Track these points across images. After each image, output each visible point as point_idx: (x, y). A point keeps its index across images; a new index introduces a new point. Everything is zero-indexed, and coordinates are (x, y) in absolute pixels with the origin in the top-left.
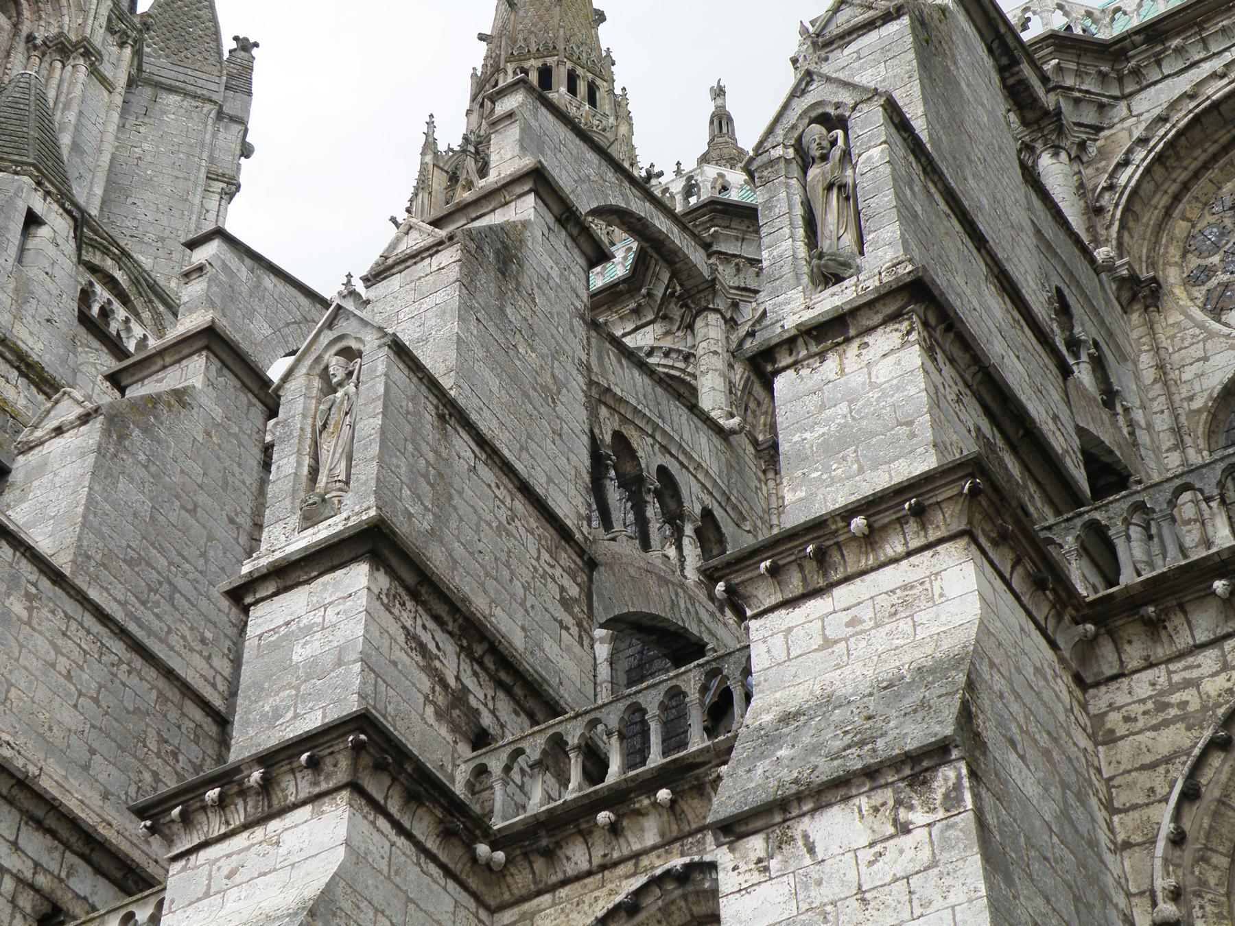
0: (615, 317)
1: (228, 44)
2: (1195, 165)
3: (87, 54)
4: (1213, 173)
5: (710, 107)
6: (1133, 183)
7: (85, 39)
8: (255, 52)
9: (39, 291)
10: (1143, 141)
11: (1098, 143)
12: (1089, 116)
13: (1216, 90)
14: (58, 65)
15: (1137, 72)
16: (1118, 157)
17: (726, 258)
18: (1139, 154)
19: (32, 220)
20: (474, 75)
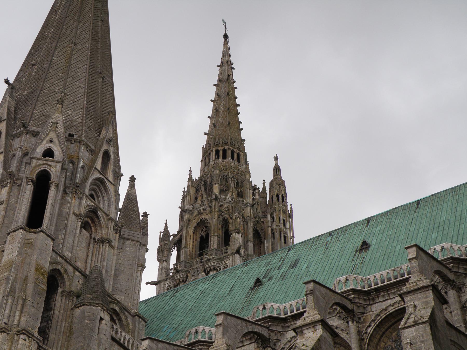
0: (245, 339)
1: (141, 214)
2: (386, 327)
3: (109, 242)
4: (390, 330)
5: (274, 164)
6: (371, 333)
7: (108, 238)
8: (148, 216)
9: (103, 341)
10: (374, 321)
11: (364, 317)
12: (361, 310)
13: (391, 310)
14: (101, 246)
15: (373, 299)
16: (368, 324)
17: (273, 331)
18: (373, 324)
19: (101, 319)
20: (203, 148)
